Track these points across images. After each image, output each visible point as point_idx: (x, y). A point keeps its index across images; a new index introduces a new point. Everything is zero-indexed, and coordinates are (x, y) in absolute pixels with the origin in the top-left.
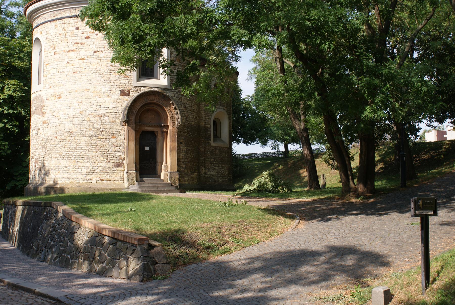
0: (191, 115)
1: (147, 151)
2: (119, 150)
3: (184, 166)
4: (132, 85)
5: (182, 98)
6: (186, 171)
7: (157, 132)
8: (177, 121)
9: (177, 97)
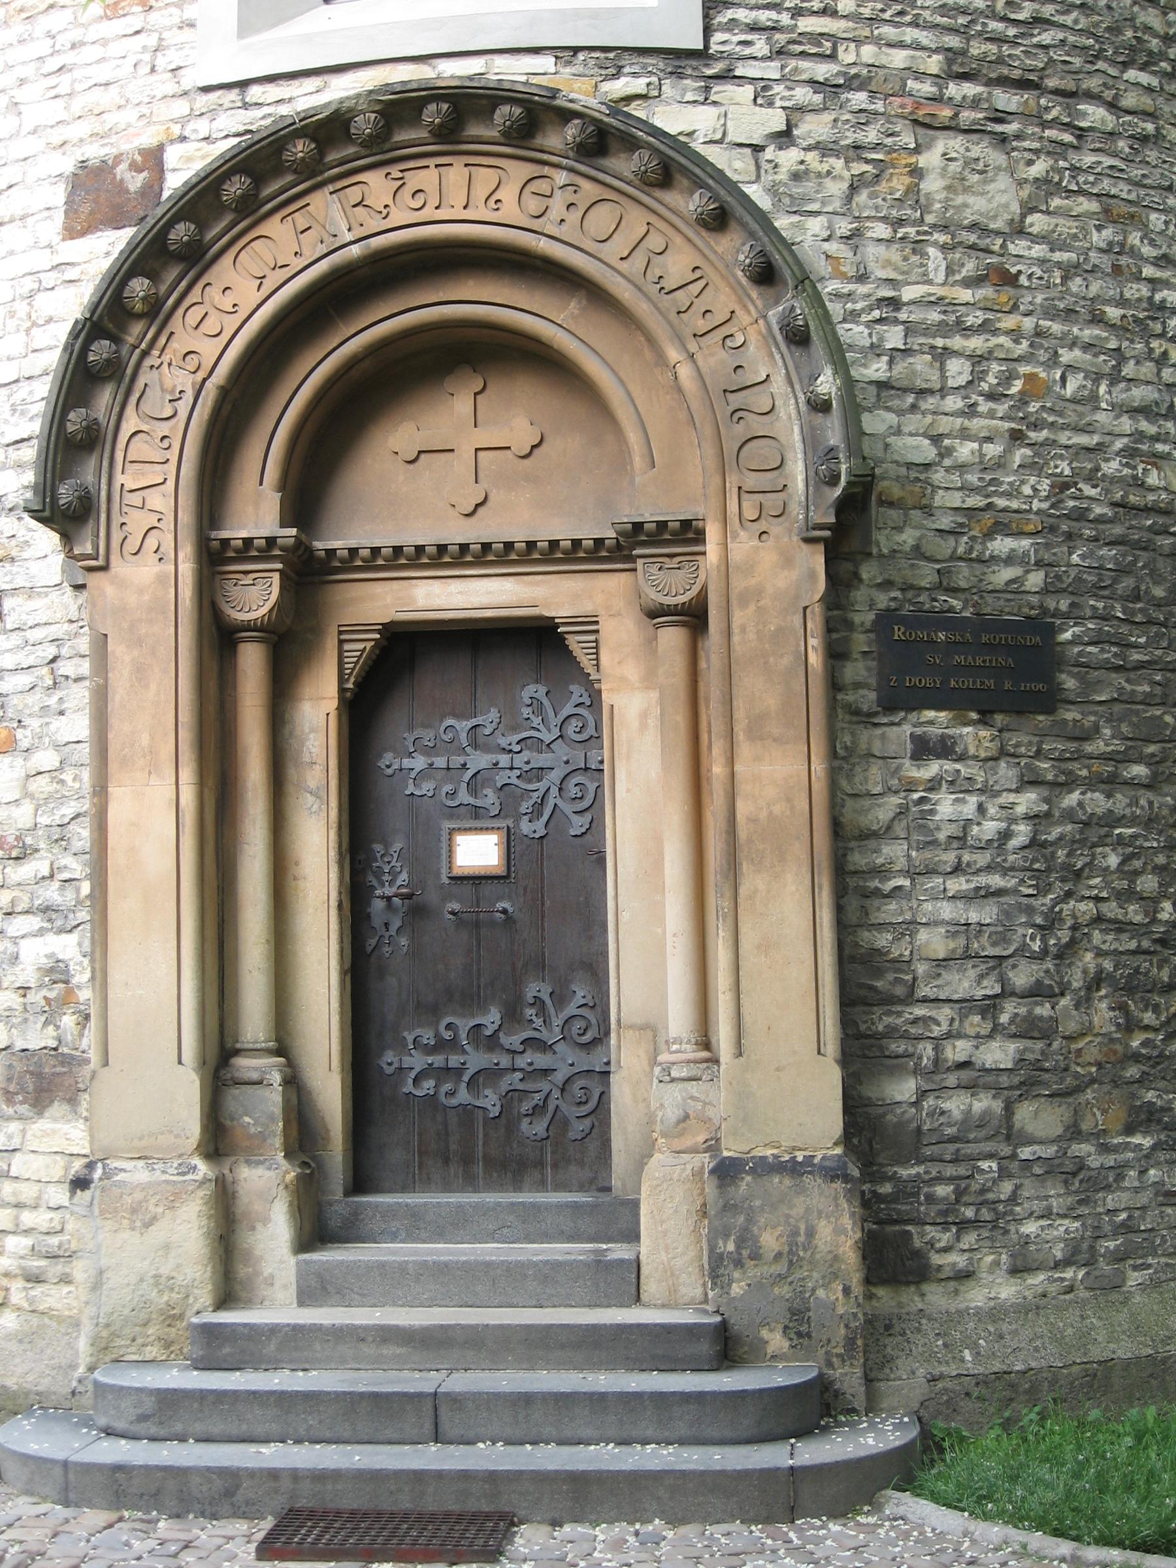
0: (1115, 378)
1: (477, 880)
2: (51, 893)
3: (999, 1054)
4: (192, 78)
5: (930, 159)
6: (1039, 1119)
7: (589, 624)
8: (811, 440)
9: (824, 149)
